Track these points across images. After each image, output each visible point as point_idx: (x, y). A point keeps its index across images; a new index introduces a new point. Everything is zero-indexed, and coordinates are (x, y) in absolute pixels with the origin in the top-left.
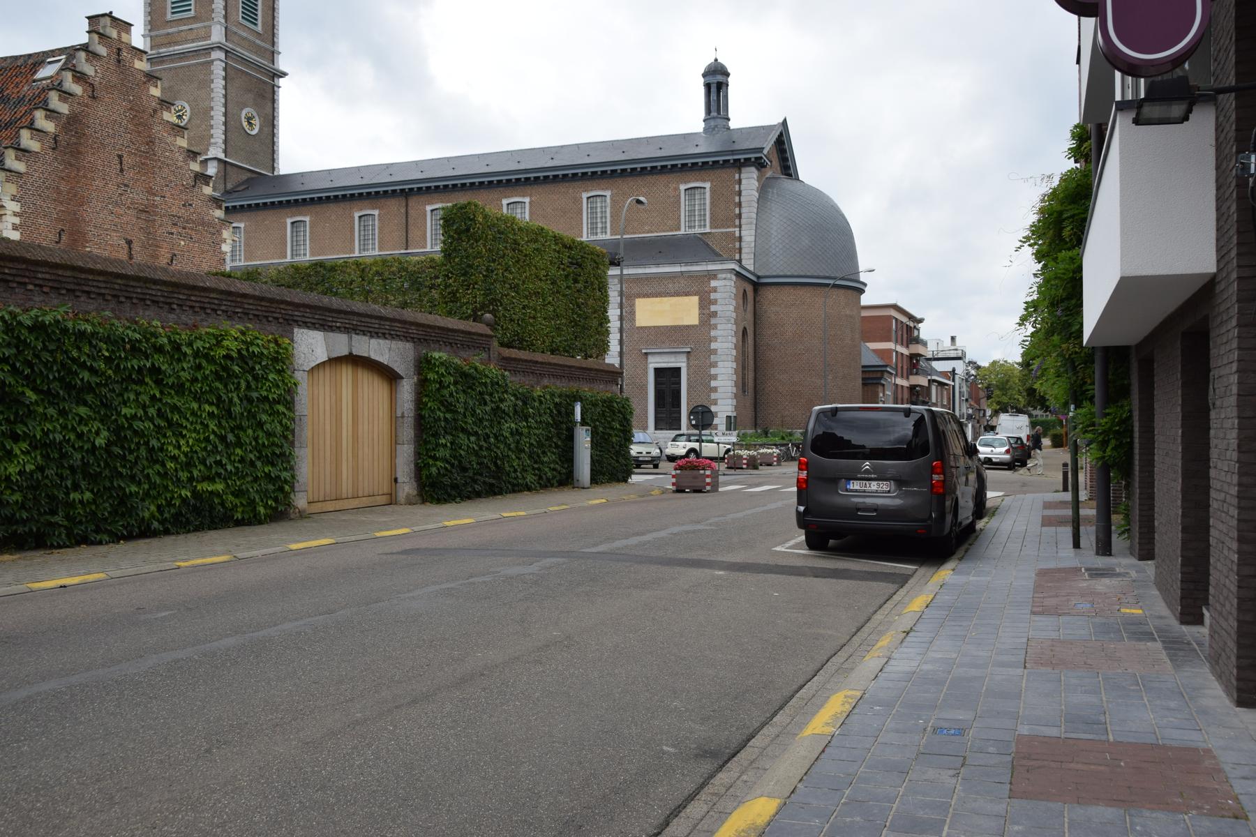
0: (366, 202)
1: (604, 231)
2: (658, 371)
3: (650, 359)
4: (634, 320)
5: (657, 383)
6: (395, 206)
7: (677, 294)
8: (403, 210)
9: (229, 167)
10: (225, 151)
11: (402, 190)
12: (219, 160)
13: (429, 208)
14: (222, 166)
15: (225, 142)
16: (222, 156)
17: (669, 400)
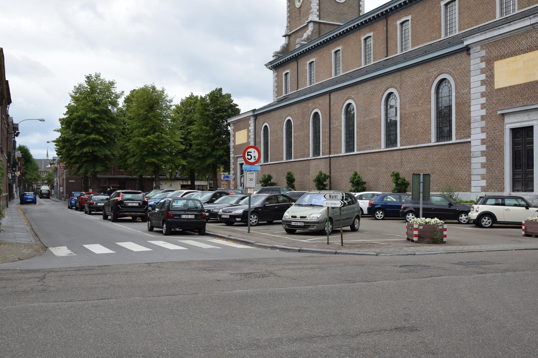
0: (367, 28)
1: (514, 10)
2: (515, 131)
3: (507, 120)
4: (493, 83)
5: (514, 144)
6: (380, 26)
7: (530, 49)
8: (385, 29)
9: (322, 26)
10: (319, 16)
11: (382, 13)
12: (315, 22)
13: (398, 22)
14: (317, 26)
15: (319, 10)
16: (317, 19)
17: (524, 160)
